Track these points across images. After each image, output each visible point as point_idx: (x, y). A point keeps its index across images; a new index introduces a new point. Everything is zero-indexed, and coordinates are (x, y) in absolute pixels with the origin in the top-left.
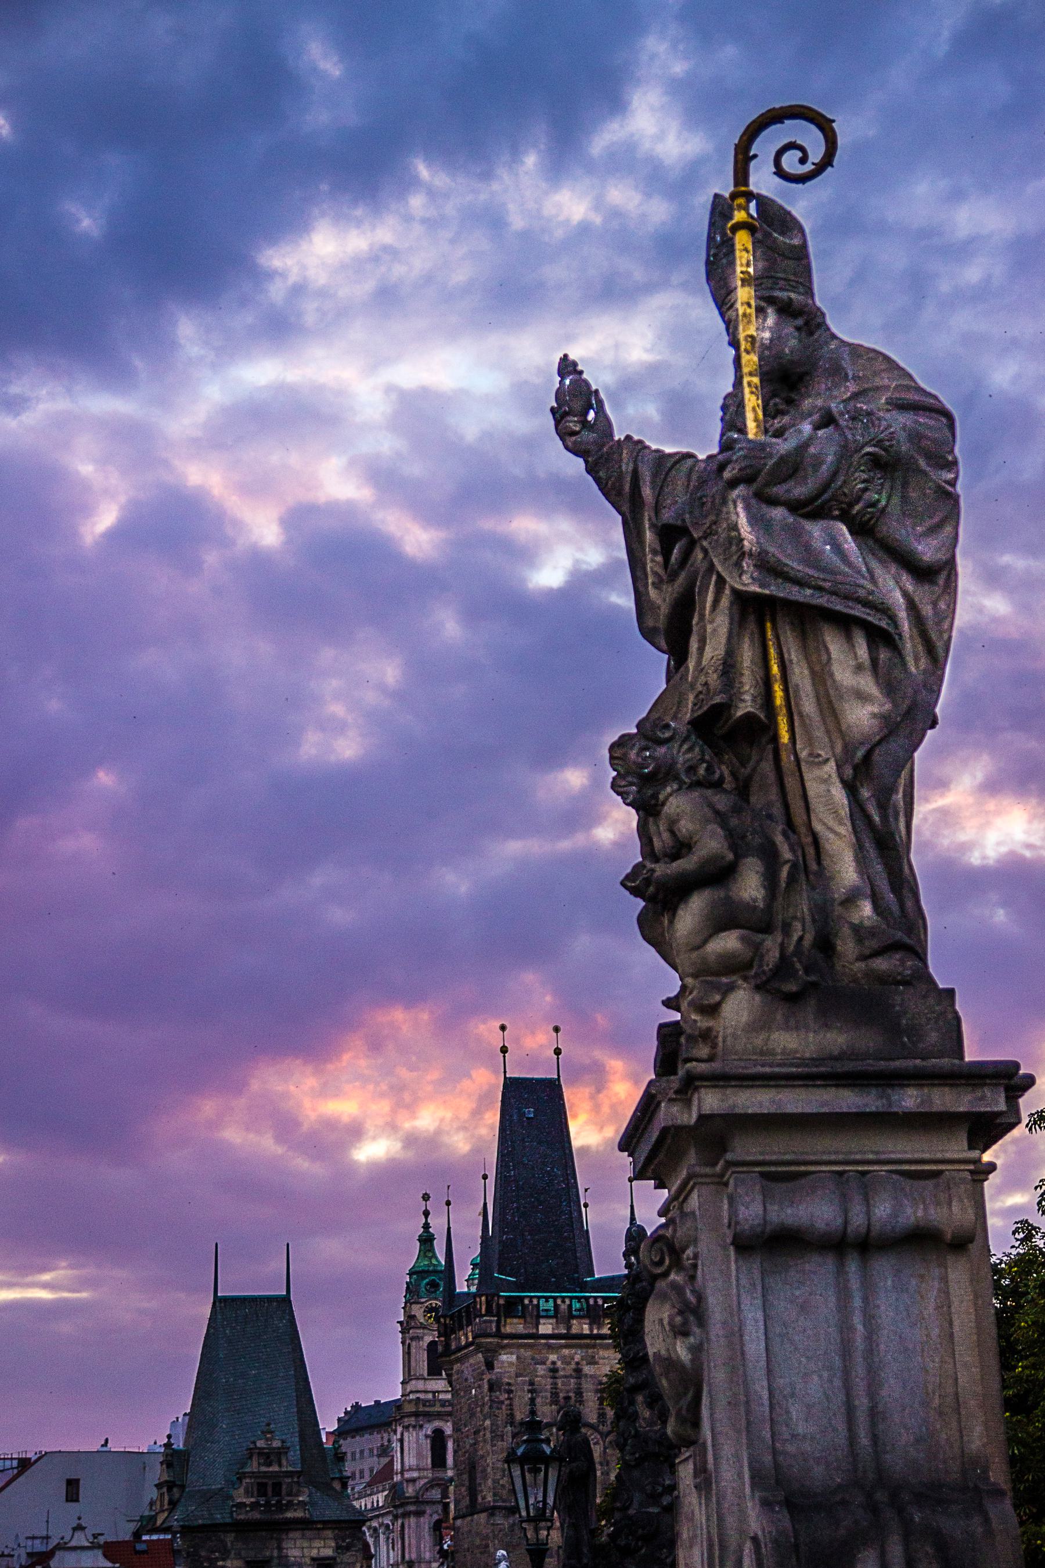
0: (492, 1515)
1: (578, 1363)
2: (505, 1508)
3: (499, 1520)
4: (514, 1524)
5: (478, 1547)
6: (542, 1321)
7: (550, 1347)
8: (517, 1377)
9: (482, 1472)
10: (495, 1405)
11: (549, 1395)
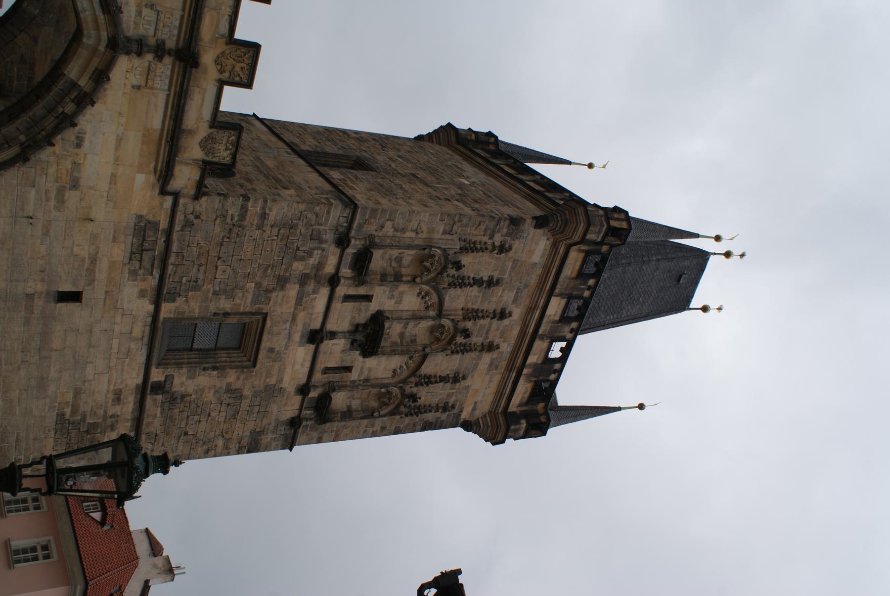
0: (346, 206)
1: (498, 347)
2: (349, 228)
3: (337, 214)
4: (321, 241)
5: (258, 159)
6: (564, 301)
7: (530, 310)
8: (514, 261)
9: (381, 185)
10: (492, 225)
11: (476, 307)
